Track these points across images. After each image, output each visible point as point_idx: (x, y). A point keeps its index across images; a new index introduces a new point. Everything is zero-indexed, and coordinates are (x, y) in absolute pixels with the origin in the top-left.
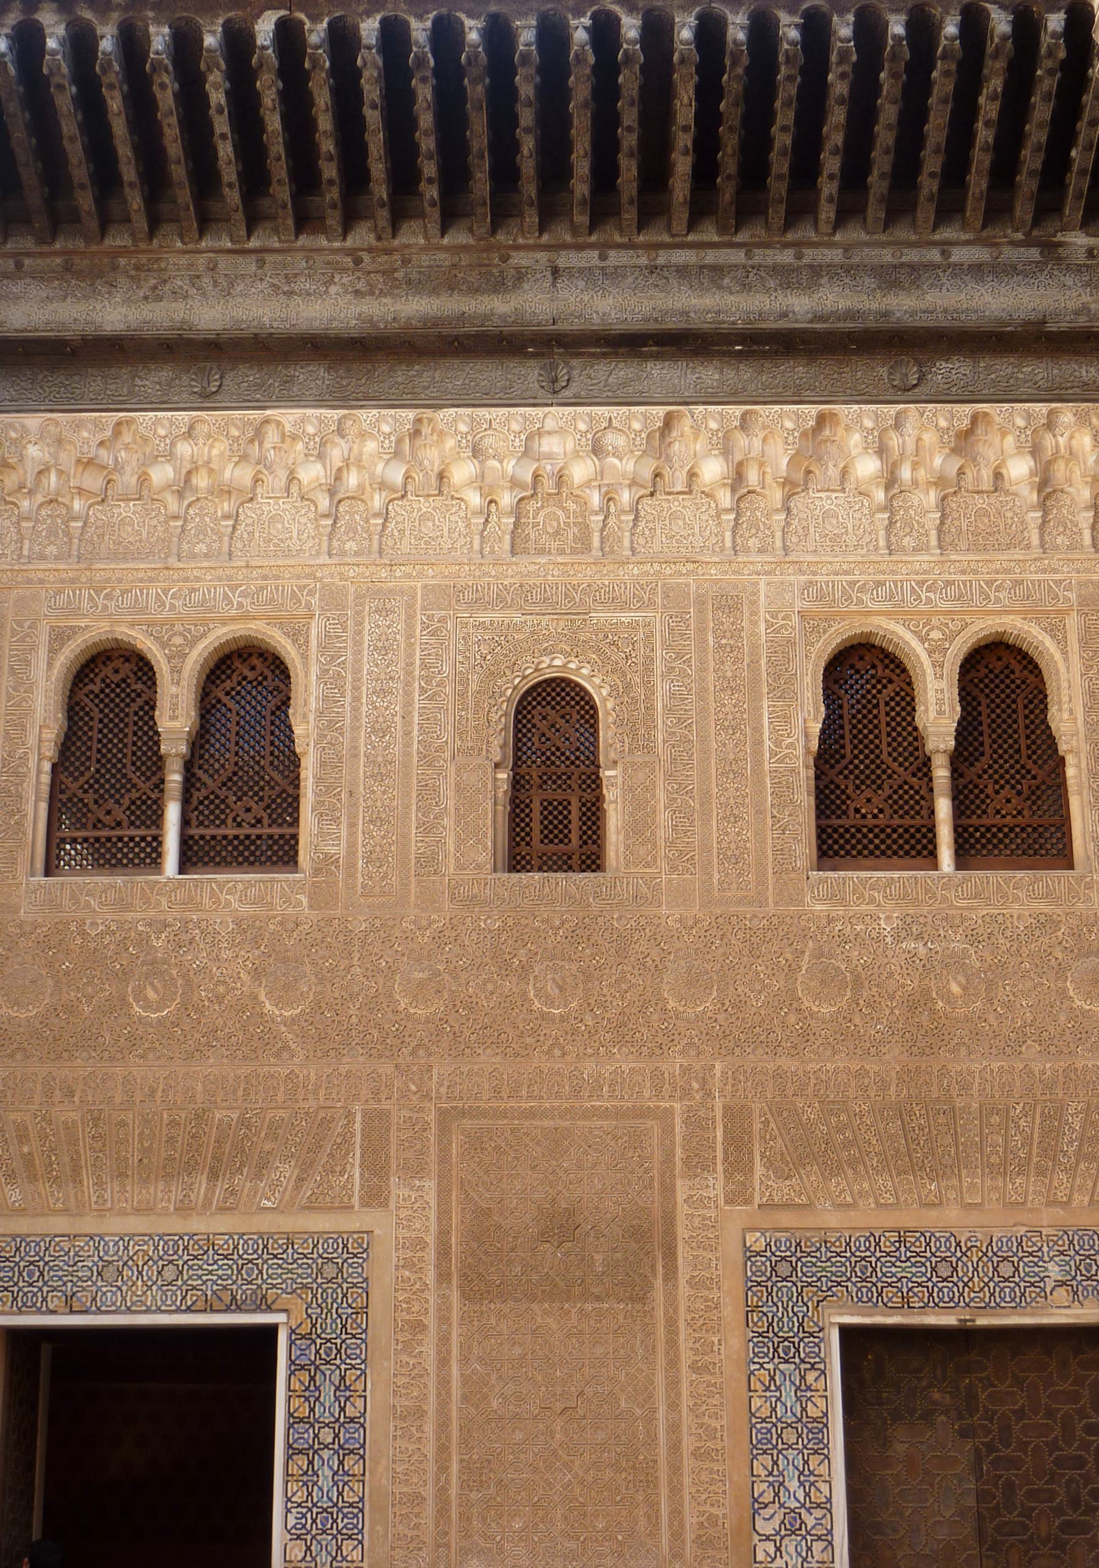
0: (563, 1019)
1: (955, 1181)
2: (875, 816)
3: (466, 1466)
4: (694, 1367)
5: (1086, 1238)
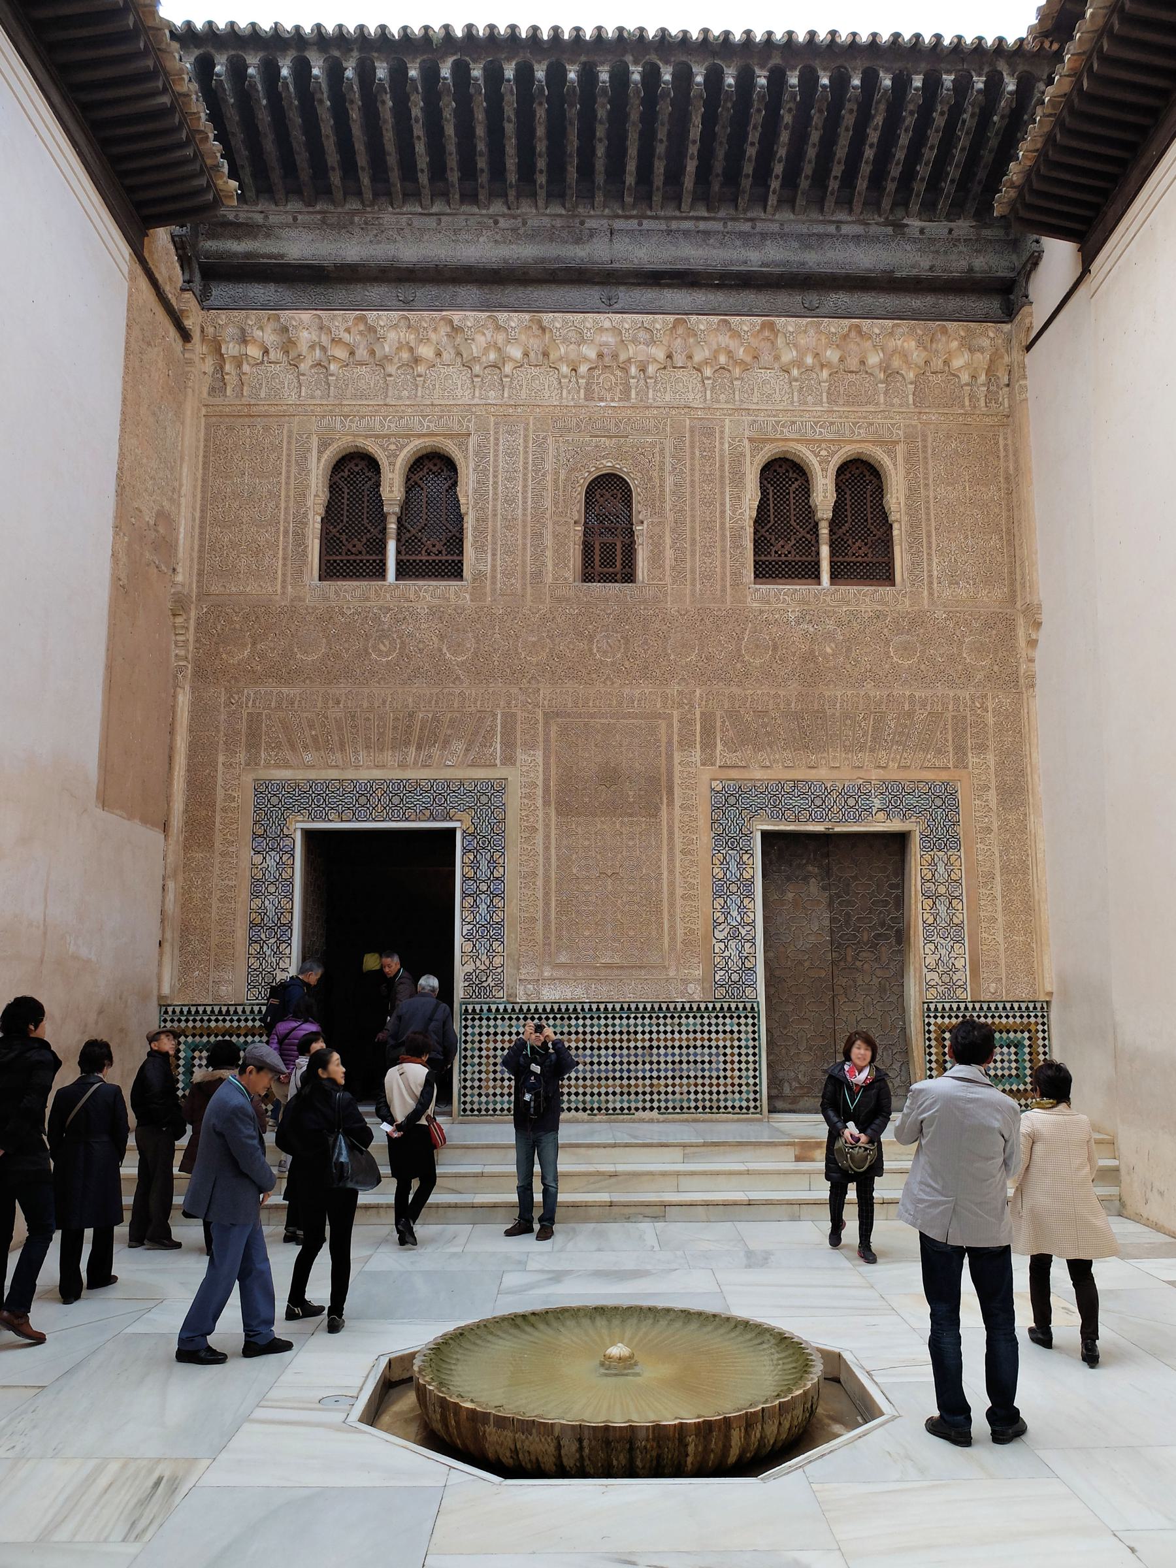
1: (825, 755)
2: (786, 556)
3: (560, 903)
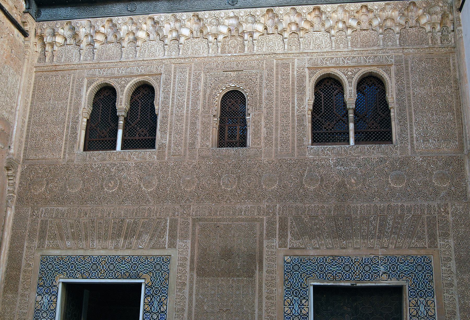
0: (231, 191)
1: (351, 241)
2: (331, 130)
4: (267, 298)
5: (393, 259)
